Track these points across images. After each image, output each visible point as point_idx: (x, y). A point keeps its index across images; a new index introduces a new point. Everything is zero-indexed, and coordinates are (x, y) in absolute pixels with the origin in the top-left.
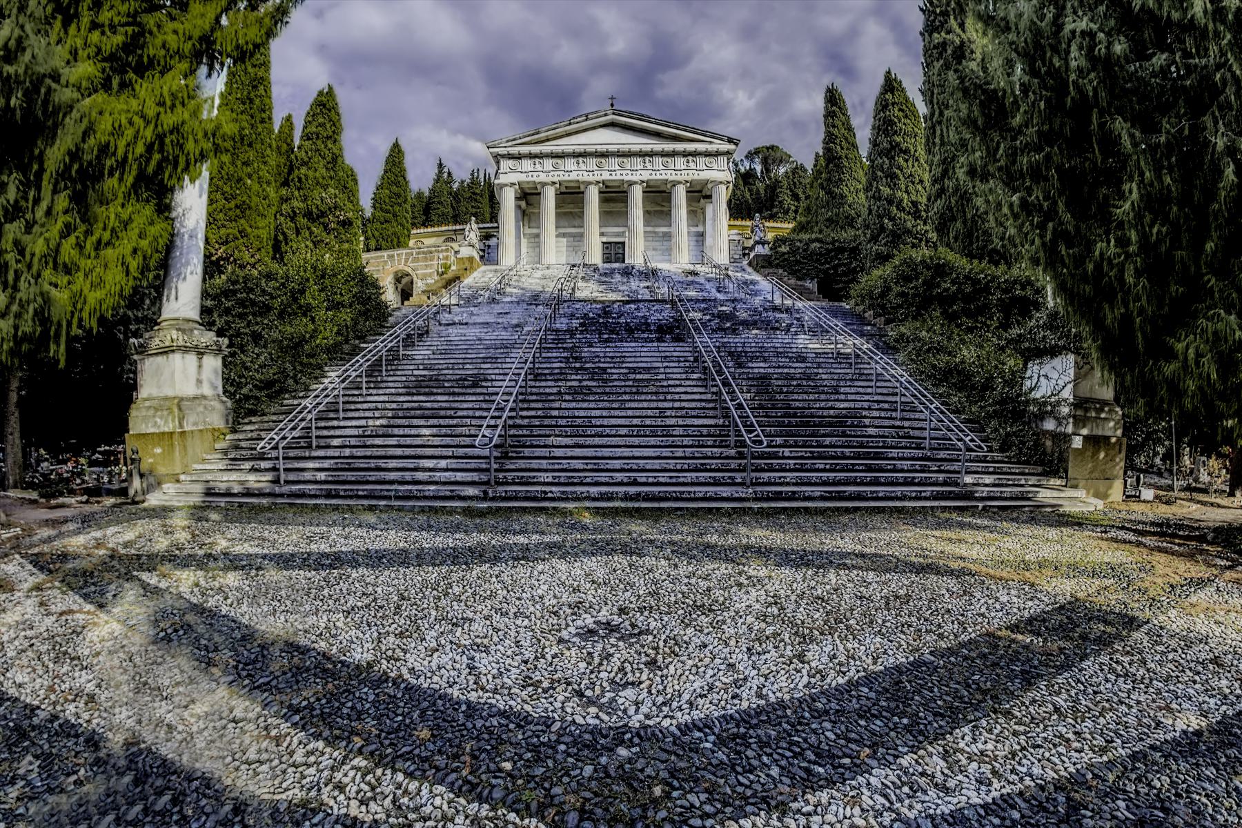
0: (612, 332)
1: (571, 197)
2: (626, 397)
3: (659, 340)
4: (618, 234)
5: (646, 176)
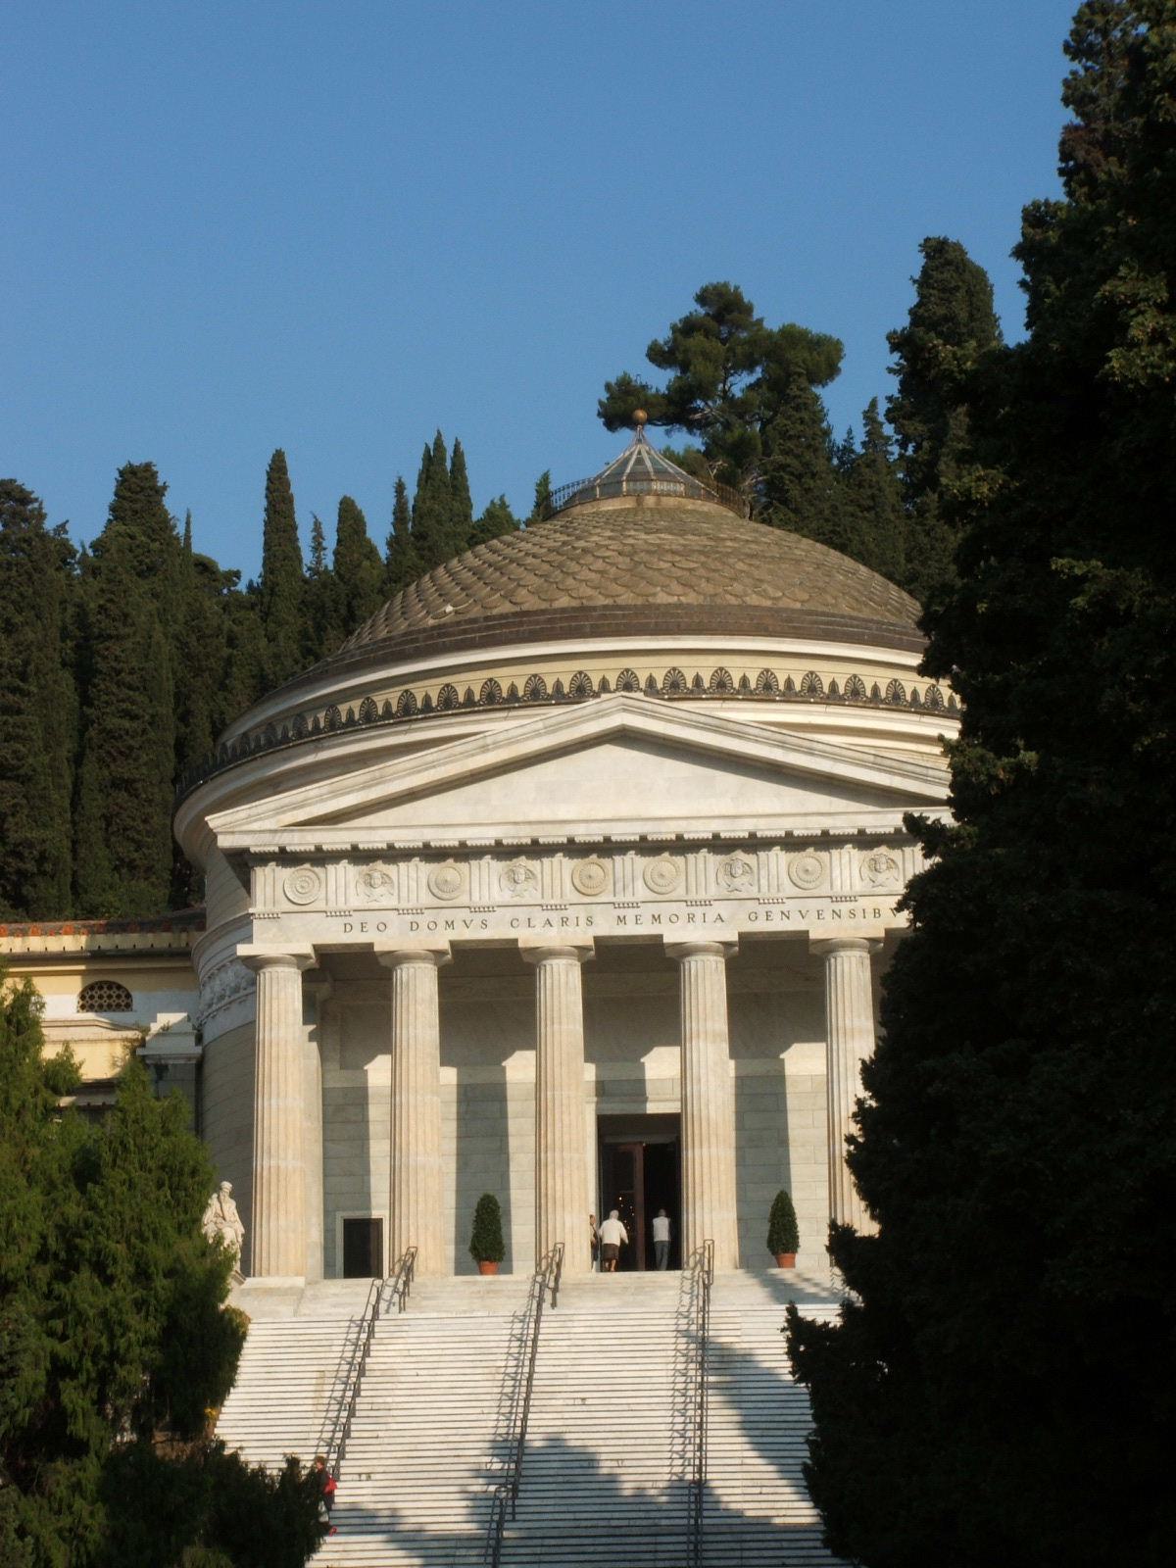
1: (489, 991)
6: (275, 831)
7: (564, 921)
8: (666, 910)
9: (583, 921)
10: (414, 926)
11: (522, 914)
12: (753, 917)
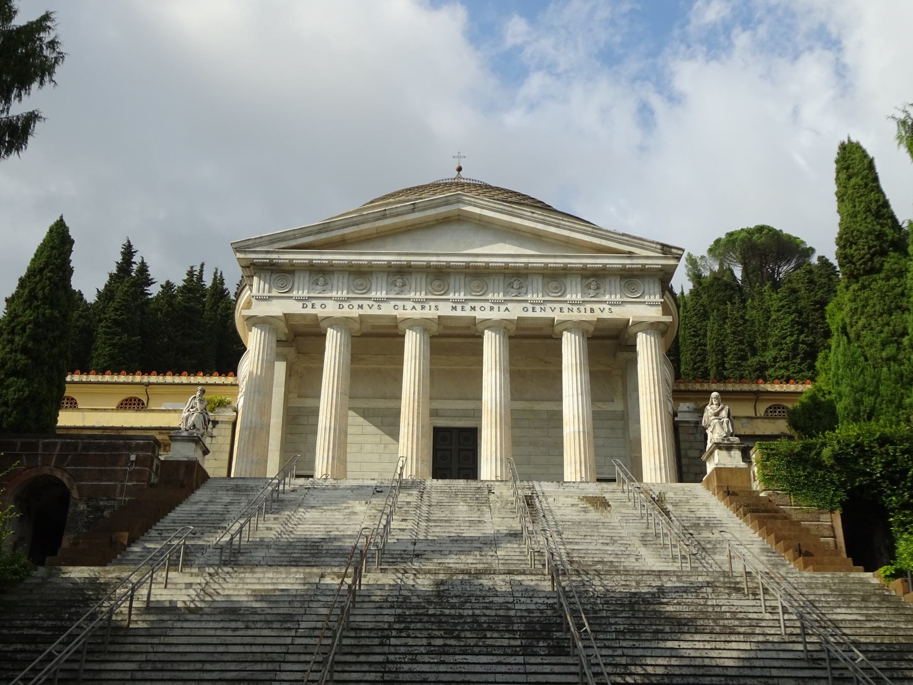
0: (450, 633)
3: (527, 651)
4: (464, 414)
5: (515, 312)
7: (423, 308)
8: (478, 305)
9: (433, 308)
11: (400, 304)
12: (525, 309)
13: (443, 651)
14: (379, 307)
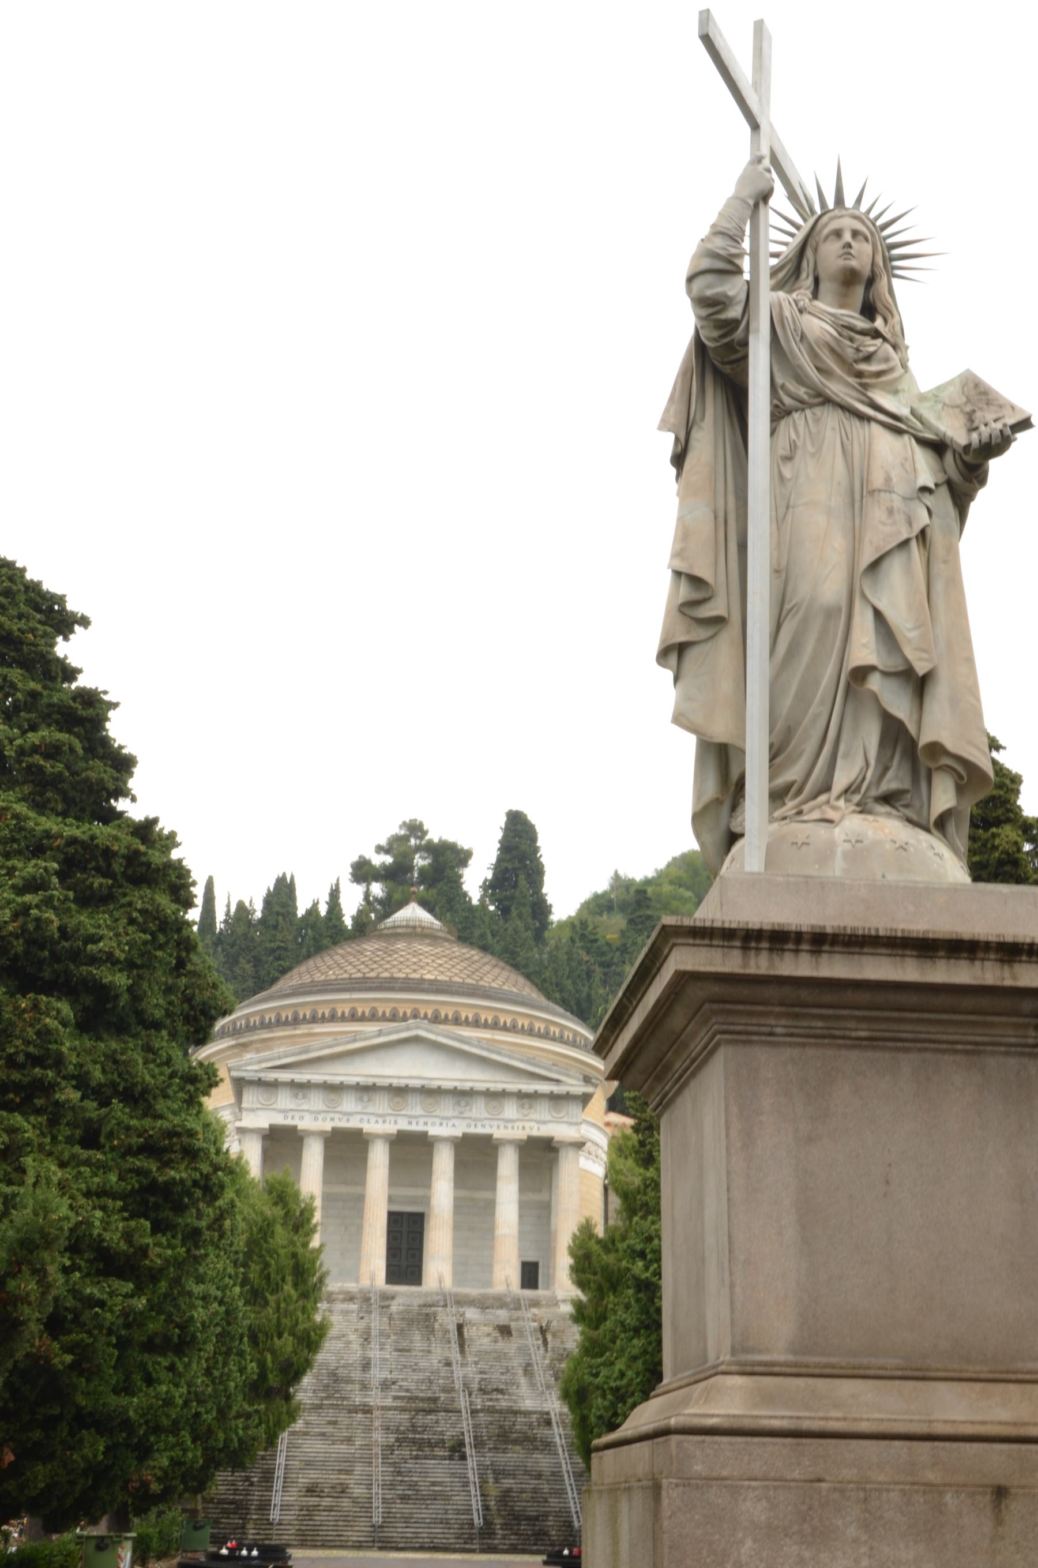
1: (346, 1148)
2: (428, 1502)
3: (451, 1458)
4: (414, 1201)
6: (256, 1071)
7: (384, 1122)
8: (430, 1120)
10: (316, 1119)
11: (365, 1117)
13: (417, 1457)
14: (348, 1120)
